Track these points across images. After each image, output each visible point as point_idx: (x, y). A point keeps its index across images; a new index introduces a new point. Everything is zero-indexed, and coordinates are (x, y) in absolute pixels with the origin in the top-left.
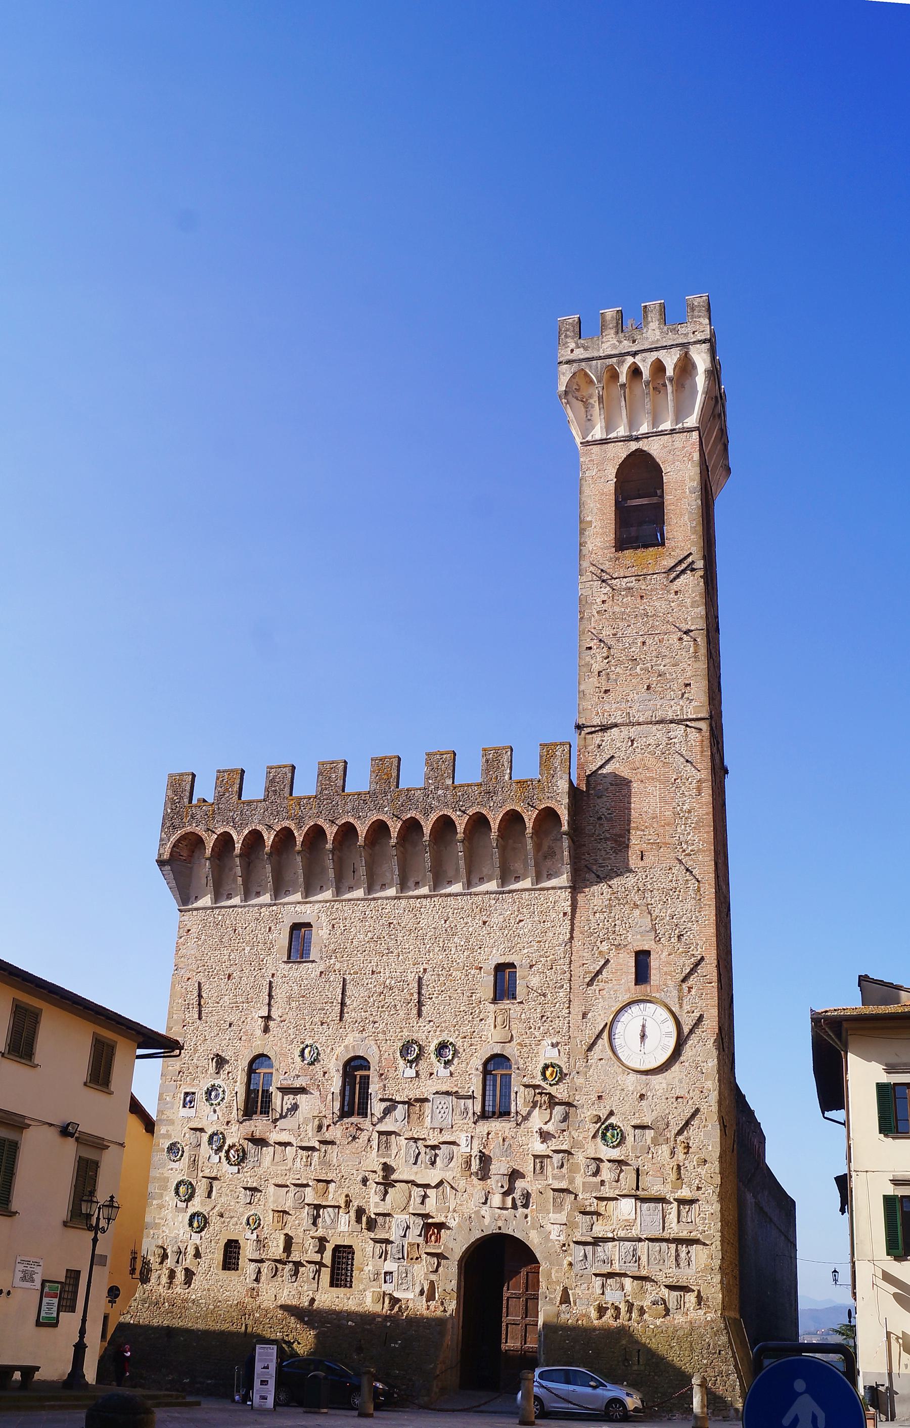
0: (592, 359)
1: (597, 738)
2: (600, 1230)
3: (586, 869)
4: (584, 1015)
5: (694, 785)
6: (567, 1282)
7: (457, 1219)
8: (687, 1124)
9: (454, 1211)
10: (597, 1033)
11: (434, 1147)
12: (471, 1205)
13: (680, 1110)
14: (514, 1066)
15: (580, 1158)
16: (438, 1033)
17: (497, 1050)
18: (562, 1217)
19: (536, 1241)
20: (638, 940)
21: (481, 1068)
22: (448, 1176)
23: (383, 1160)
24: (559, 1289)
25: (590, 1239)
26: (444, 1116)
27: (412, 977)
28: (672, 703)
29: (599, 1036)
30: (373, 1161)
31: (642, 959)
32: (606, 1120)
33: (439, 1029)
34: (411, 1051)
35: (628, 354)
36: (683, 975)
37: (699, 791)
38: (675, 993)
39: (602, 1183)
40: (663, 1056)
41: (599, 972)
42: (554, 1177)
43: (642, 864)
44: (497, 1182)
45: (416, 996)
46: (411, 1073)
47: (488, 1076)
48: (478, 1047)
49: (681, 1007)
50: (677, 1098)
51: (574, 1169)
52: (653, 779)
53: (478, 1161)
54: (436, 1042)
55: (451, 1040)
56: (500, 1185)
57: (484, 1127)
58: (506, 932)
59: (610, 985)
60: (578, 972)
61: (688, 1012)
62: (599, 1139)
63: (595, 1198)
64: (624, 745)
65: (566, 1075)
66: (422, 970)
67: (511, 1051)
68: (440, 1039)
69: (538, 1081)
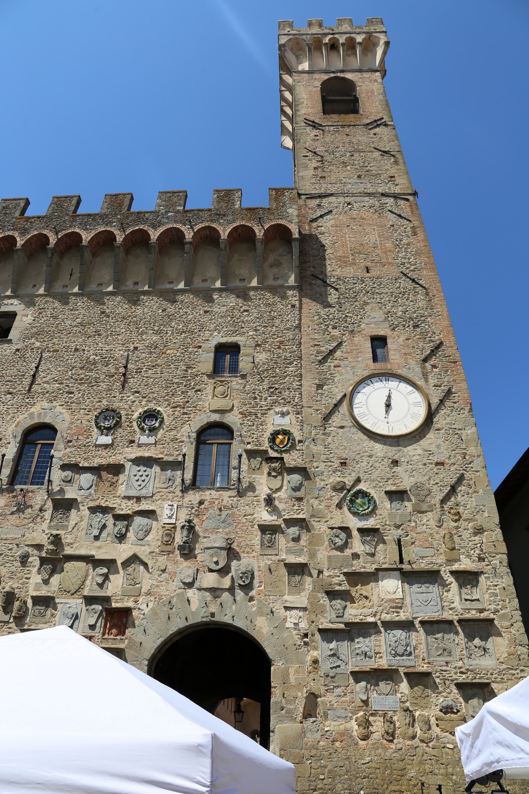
0: (304, 34)
1: (317, 201)
2: (354, 613)
3: (312, 277)
4: (320, 387)
5: (409, 229)
6: (314, 686)
7: (151, 605)
8: (453, 490)
9: (148, 593)
10: (334, 402)
11: (127, 518)
12: (171, 588)
13: (442, 476)
14: (235, 433)
15: (321, 528)
16: (143, 403)
17: (216, 417)
18: (301, 600)
19: (265, 631)
20: (373, 328)
21: (194, 435)
22: (143, 552)
23: (55, 532)
24: (302, 694)
25: (342, 626)
26: (143, 484)
27: (120, 353)
28: (381, 185)
29: (337, 406)
30: (41, 533)
31: (379, 342)
32: (353, 486)
33: (145, 399)
34: (109, 420)
35: (329, 34)
36: (423, 356)
37: (415, 234)
38: (418, 369)
39: (356, 556)
40: (413, 424)
41: (332, 352)
42: (289, 551)
43: (368, 275)
44: (212, 556)
45: (122, 370)
46: (106, 440)
47: (202, 447)
48: (192, 416)
49: (426, 381)
50: (437, 464)
51: (314, 542)
52: (371, 225)
53: (185, 532)
54: (141, 410)
55: (159, 409)
56: (215, 559)
57: (193, 497)
58: (229, 319)
59: (346, 363)
60: (307, 350)
61: (434, 386)
62: (345, 509)
63: (345, 574)
64: (341, 205)
65: (300, 441)
66: (132, 348)
67: (233, 419)
68: (146, 408)
69: (266, 445)
